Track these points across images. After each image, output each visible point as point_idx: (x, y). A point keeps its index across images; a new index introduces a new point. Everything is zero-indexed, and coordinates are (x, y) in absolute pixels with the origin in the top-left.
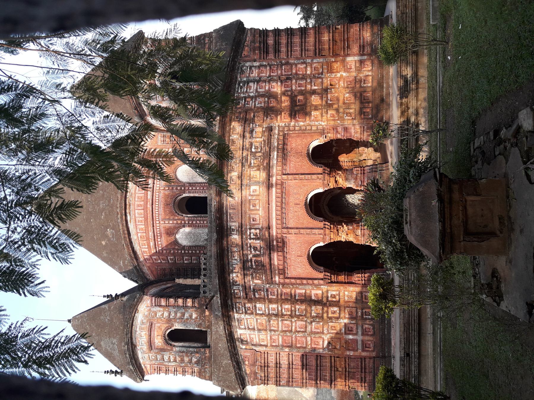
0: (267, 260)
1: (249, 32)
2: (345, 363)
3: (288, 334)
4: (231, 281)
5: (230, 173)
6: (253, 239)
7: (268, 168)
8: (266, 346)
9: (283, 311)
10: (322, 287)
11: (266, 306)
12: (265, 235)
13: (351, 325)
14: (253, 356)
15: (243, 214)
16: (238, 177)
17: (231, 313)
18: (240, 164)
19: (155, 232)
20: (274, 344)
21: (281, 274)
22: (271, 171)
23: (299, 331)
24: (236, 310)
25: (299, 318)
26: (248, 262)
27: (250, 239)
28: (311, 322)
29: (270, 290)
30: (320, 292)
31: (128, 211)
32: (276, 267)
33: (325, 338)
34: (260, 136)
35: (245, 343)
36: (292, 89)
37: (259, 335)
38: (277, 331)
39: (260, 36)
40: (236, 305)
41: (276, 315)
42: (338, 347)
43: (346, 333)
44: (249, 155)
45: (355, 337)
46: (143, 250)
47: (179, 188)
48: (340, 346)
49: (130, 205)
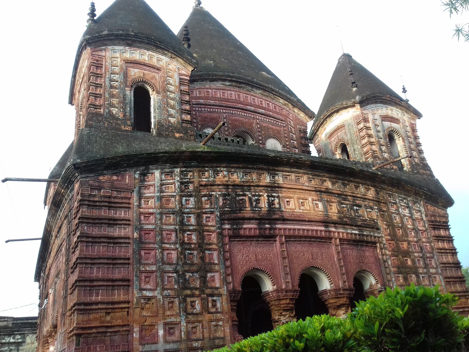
0: (247, 215)
1: (445, 212)
2: (119, 326)
3: (158, 239)
4: (218, 169)
5: (330, 181)
6: (268, 200)
8: (139, 206)
9: (188, 233)
10: (226, 288)
11: (193, 210)
12: (275, 214)
13: (177, 333)
14: (125, 186)
16: (327, 189)
17: (181, 164)
18: (340, 192)
19: (214, 107)
20: (142, 218)
21: (233, 232)
22: (340, 226)
23: (163, 255)
24: (184, 171)
25: (181, 253)
26: (243, 192)
27: (268, 196)
28: (176, 272)
29: (212, 216)
30: (218, 285)
31: (234, 84)
32: (241, 226)
33: (156, 292)
34: (369, 216)
35: (143, 178)
36: (414, 252)
37: (152, 197)
38: (161, 223)
39: (444, 222)
40: (190, 171)
41: (182, 223)
43: (165, 324)
44: (350, 203)
45: (161, 340)
46: (195, 91)
47: (260, 138)
48: (146, 316)
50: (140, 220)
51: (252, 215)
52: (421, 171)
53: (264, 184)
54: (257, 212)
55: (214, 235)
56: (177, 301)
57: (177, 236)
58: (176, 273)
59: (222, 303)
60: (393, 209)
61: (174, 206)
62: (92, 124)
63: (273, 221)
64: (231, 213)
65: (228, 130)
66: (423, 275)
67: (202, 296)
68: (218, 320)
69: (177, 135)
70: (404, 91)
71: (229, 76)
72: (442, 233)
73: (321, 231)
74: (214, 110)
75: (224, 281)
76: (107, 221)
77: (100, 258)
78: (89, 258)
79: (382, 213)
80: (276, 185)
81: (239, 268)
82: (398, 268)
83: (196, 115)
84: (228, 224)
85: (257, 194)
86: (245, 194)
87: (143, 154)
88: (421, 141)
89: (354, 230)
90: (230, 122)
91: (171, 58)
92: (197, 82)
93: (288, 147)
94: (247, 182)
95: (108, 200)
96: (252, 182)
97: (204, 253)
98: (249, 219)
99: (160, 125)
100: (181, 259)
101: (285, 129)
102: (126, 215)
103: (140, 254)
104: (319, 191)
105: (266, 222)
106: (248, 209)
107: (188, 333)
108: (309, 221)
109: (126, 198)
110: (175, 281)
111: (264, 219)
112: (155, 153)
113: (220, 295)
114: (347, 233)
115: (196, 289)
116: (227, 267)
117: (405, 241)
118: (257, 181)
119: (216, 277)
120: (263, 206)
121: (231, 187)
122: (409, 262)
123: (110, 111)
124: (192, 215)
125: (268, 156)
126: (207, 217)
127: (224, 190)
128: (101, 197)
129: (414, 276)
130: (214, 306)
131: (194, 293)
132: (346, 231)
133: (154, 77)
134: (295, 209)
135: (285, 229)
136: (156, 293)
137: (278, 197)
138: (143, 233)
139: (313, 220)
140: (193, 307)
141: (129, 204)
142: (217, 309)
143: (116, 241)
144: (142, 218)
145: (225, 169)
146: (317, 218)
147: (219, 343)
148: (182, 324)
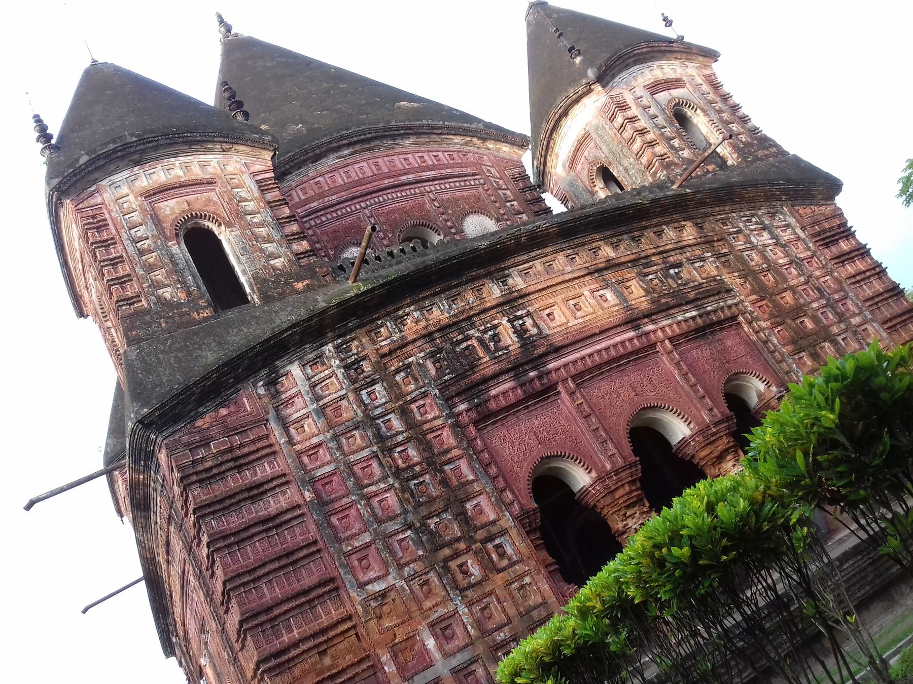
0: (489, 371)
1: (833, 207)
2: (353, 665)
3: (350, 483)
4: (400, 312)
5: (607, 244)
6: (513, 327)
7: (658, 310)
8: (291, 442)
9: (399, 449)
13: (459, 631)
15: (544, 293)
16: (609, 260)
17: (330, 334)
18: (633, 257)
19: (342, 205)
20: (305, 459)
21: (478, 412)
22: (660, 316)
23: (372, 509)
25: (403, 491)
26: (463, 333)
28: (410, 526)
29: (428, 401)
30: (492, 517)
31: (358, 147)
32: (486, 396)
33: (390, 578)
34: (704, 275)
35: (273, 390)
36: (810, 303)
38: (344, 454)
39: (839, 226)
40: (352, 340)
41: (380, 438)
42: (387, 624)
43: (432, 626)
45: (437, 655)
47: (449, 224)
48: (392, 628)
49: (369, 149)
50: (303, 466)
51: (496, 367)
52: (760, 153)
53: (494, 303)
54: (503, 357)
55: (446, 433)
56: (433, 577)
57: (381, 464)
58: (409, 528)
59: (515, 544)
60: (740, 244)
61: (352, 413)
62: (137, 335)
63: (538, 361)
64: (459, 381)
65: (386, 235)
66: (843, 336)
67: (473, 547)
68: (521, 577)
69: (299, 286)
70: (668, 22)
71: (343, 137)
72: (844, 246)
73: (631, 340)
74: (344, 211)
75: (501, 504)
76: (246, 495)
77: (264, 564)
78: (244, 573)
79: (723, 259)
80: (515, 294)
81: (517, 469)
82: (793, 342)
83: (315, 234)
84: (462, 402)
85: (489, 325)
86: (468, 335)
87: (254, 347)
88: (736, 99)
89: (687, 311)
90: (382, 220)
91: (224, 151)
92: (291, 173)
93: (506, 217)
94: (462, 313)
95: (229, 456)
96: (471, 308)
97: (442, 471)
98: (495, 376)
99: (259, 281)
100: (407, 500)
101: (486, 187)
102: (274, 467)
103: (330, 524)
104: (595, 271)
105: (527, 368)
106: (485, 360)
107: (478, 623)
108: (601, 332)
109: (260, 439)
110: (414, 543)
111: (522, 365)
112: (275, 336)
113: (504, 532)
114: (679, 323)
115: (458, 540)
116: (494, 479)
117: (785, 290)
118: (478, 302)
119: (482, 504)
120: (509, 342)
121: (437, 335)
122: (809, 324)
123: (159, 298)
124: (392, 416)
125: (477, 250)
126: (419, 408)
127: (427, 346)
128: (215, 456)
129: (827, 344)
130: (502, 555)
131: (457, 549)
132: (675, 320)
133: (209, 201)
134: (568, 322)
135: (565, 366)
136: (391, 580)
137: (529, 314)
138: (319, 486)
139: (608, 326)
140: (466, 573)
141: (270, 445)
142: (509, 559)
143: (278, 521)
144: (305, 459)
145: (412, 308)
146: (614, 321)
147: (540, 615)
148: (461, 613)
